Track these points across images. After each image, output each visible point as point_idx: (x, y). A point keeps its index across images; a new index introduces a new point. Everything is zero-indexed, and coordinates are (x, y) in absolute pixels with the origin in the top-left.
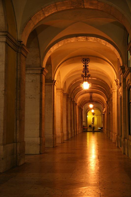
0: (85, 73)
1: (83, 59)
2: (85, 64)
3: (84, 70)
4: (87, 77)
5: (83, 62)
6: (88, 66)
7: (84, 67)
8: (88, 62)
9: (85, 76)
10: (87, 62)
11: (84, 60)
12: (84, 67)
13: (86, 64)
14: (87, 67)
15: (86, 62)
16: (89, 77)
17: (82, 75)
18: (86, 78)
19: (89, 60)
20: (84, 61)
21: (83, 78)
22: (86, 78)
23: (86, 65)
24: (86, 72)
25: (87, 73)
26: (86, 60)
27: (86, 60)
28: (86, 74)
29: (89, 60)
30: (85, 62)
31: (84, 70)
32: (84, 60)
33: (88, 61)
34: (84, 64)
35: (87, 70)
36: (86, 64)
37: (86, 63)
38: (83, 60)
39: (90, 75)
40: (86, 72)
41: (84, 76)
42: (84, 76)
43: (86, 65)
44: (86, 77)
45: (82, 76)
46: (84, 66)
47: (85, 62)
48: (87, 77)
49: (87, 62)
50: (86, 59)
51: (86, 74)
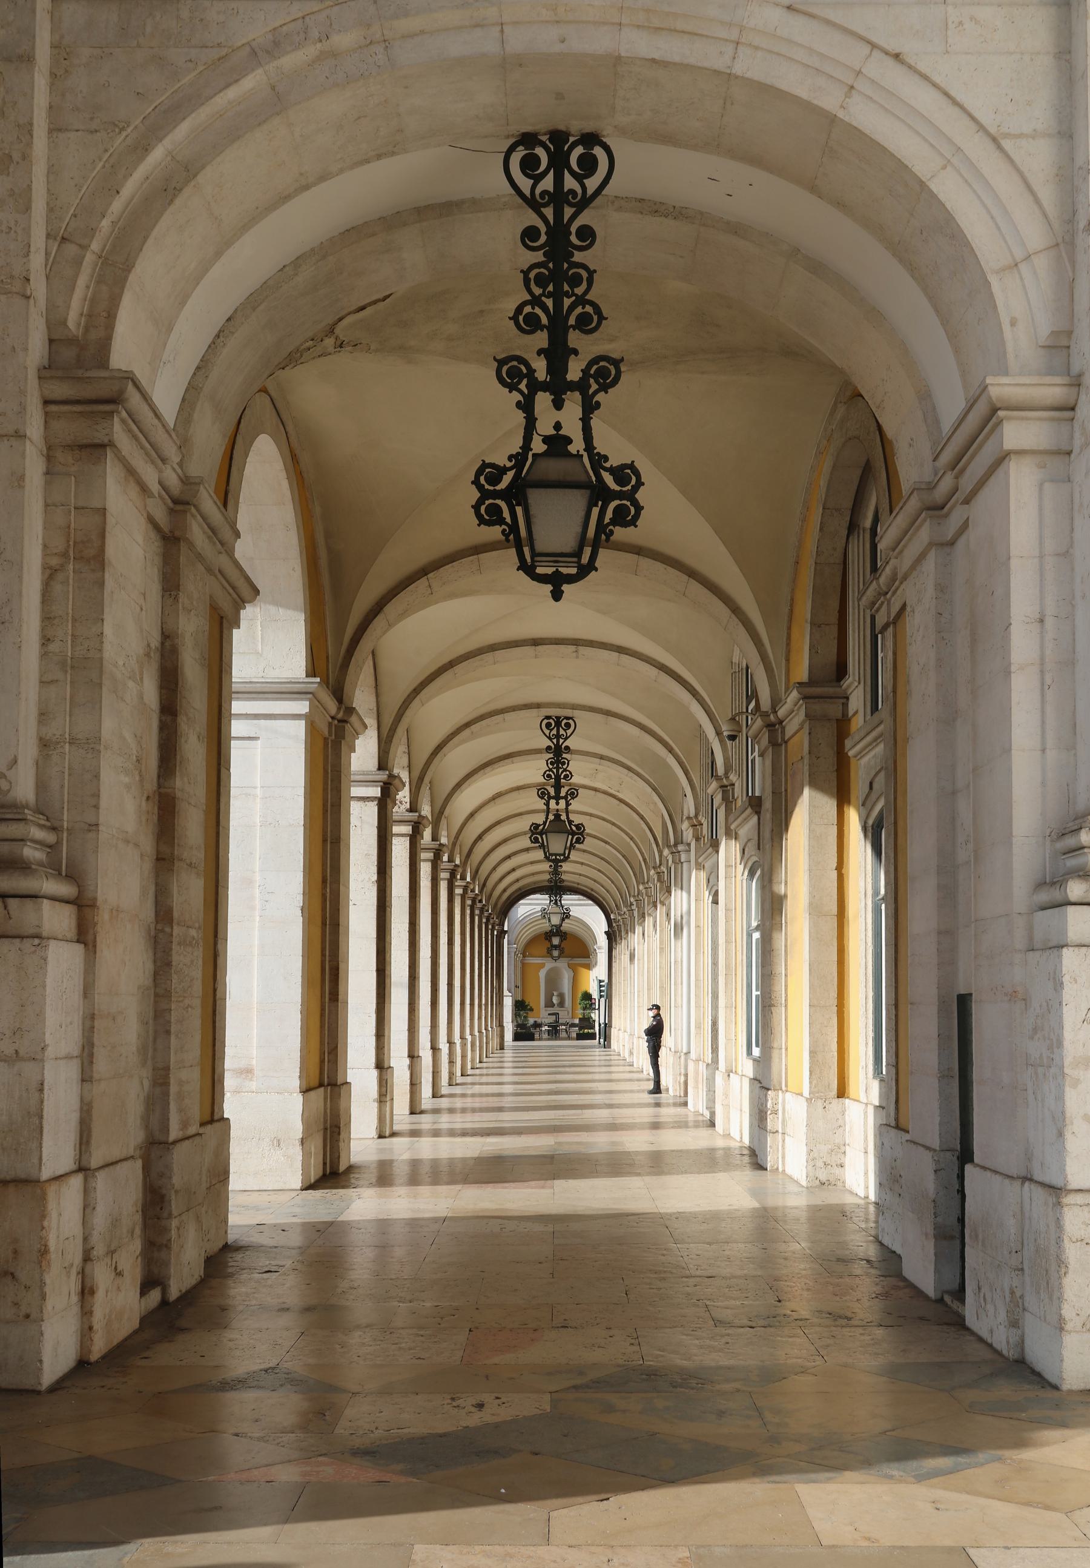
0: (541, 339)
1: (528, 139)
2: (549, 212)
3: (535, 301)
4: (581, 386)
6: (587, 234)
7: (539, 257)
8: (592, 183)
9: (541, 374)
10: (570, 183)
11: (540, 152)
12: (539, 257)
13: (558, 214)
14: (578, 257)
15: (559, 181)
16: (604, 388)
17: (501, 363)
18: (558, 405)
19: (598, 151)
20: (529, 165)
21: (527, 406)
22: (558, 405)
23: (558, 231)
24: (558, 329)
25: (574, 338)
26: (558, 162)
27: (558, 162)
28: (558, 354)
29: (598, 151)
31: (535, 301)
32: (540, 152)
33: (589, 165)
34: (533, 203)
35: (581, 301)
36: (568, 212)
37: (558, 197)
39: (616, 363)
40: (558, 329)
41: (535, 386)
42: (535, 386)
43: (558, 231)
44: (557, 798)
46: (529, 235)
47: (547, 183)
48: (581, 386)
49: (570, 183)
50: (558, 137)
51: (558, 354)
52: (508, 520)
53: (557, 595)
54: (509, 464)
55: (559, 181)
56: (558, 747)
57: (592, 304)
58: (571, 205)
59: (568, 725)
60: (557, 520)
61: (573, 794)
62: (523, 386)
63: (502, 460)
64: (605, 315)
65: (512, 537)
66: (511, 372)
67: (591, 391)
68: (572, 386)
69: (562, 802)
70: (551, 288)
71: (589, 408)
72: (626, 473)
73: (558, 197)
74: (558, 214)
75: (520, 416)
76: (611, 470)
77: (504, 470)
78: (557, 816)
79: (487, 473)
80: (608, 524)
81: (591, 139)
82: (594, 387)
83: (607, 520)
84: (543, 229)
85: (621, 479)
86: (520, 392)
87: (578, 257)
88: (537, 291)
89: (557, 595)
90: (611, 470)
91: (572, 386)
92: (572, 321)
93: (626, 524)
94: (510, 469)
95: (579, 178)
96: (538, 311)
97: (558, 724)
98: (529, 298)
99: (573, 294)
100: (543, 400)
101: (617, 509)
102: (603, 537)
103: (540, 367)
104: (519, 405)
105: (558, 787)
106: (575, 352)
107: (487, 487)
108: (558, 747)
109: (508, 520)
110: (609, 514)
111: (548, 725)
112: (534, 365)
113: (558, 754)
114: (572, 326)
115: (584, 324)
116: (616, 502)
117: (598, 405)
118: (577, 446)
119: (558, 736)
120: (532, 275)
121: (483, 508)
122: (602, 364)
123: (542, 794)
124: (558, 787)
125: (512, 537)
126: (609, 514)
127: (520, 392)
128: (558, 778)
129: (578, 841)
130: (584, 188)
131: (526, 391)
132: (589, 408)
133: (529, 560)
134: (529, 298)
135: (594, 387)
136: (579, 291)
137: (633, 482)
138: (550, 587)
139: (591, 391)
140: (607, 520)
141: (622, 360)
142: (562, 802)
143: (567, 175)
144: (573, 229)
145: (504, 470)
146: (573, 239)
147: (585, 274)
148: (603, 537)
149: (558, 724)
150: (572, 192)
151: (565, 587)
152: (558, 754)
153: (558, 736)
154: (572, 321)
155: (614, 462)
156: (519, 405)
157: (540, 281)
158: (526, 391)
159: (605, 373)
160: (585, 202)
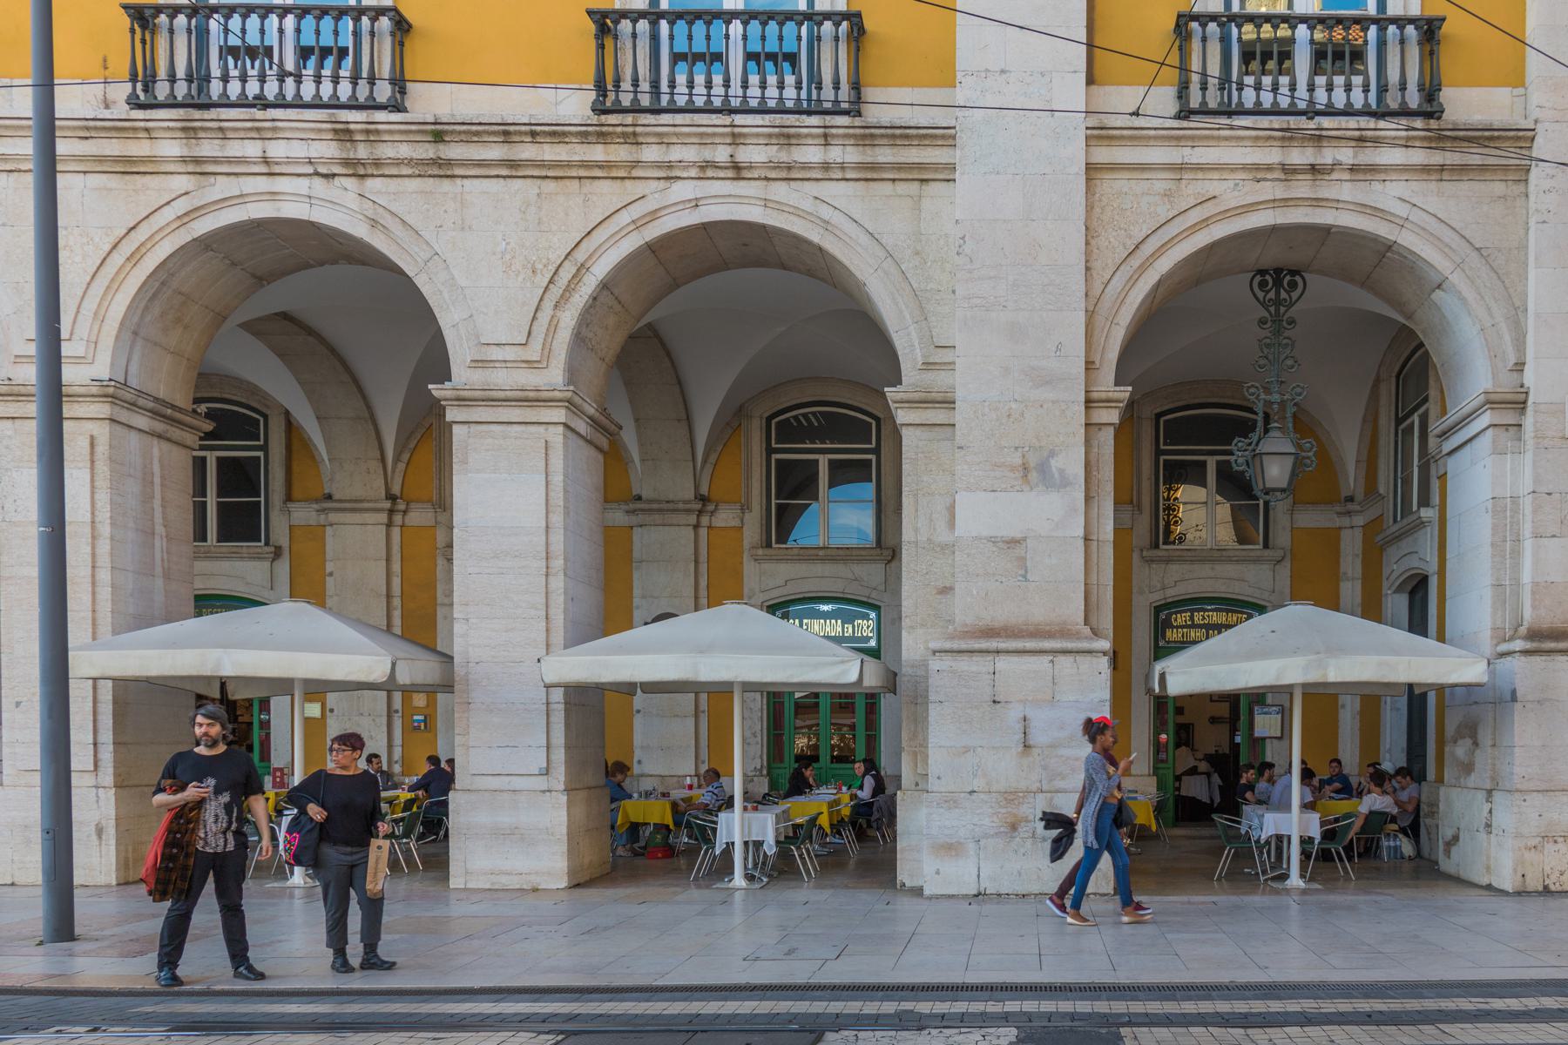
2: (1272, 309)
5: (1261, 295)
6: (1292, 322)
8: (1295, 295)
10: (1283, 295)
11: (1268, 277)
13: (1277, 310)
15: (1278, 293)
19: (1298, 278)
20: (1263, 285)
23: (1277, 319)
26: (1278, 283)
27: (1278, 283)
29: (1298, 278)
30: (1272, 295)
33: (1293, 285)
34: (1263, 304)
36: (1282, 309)
37: (1278, 302)
38: (1258, 278)
46: (1262, 322)
47: (1272, 295)
49: (1283, 295)
55: (1278, 293)
73: (1278, 302)
74: (1277, 310)
81: (1293, 273)
95: (1288, 292)
160: (1292, 304)
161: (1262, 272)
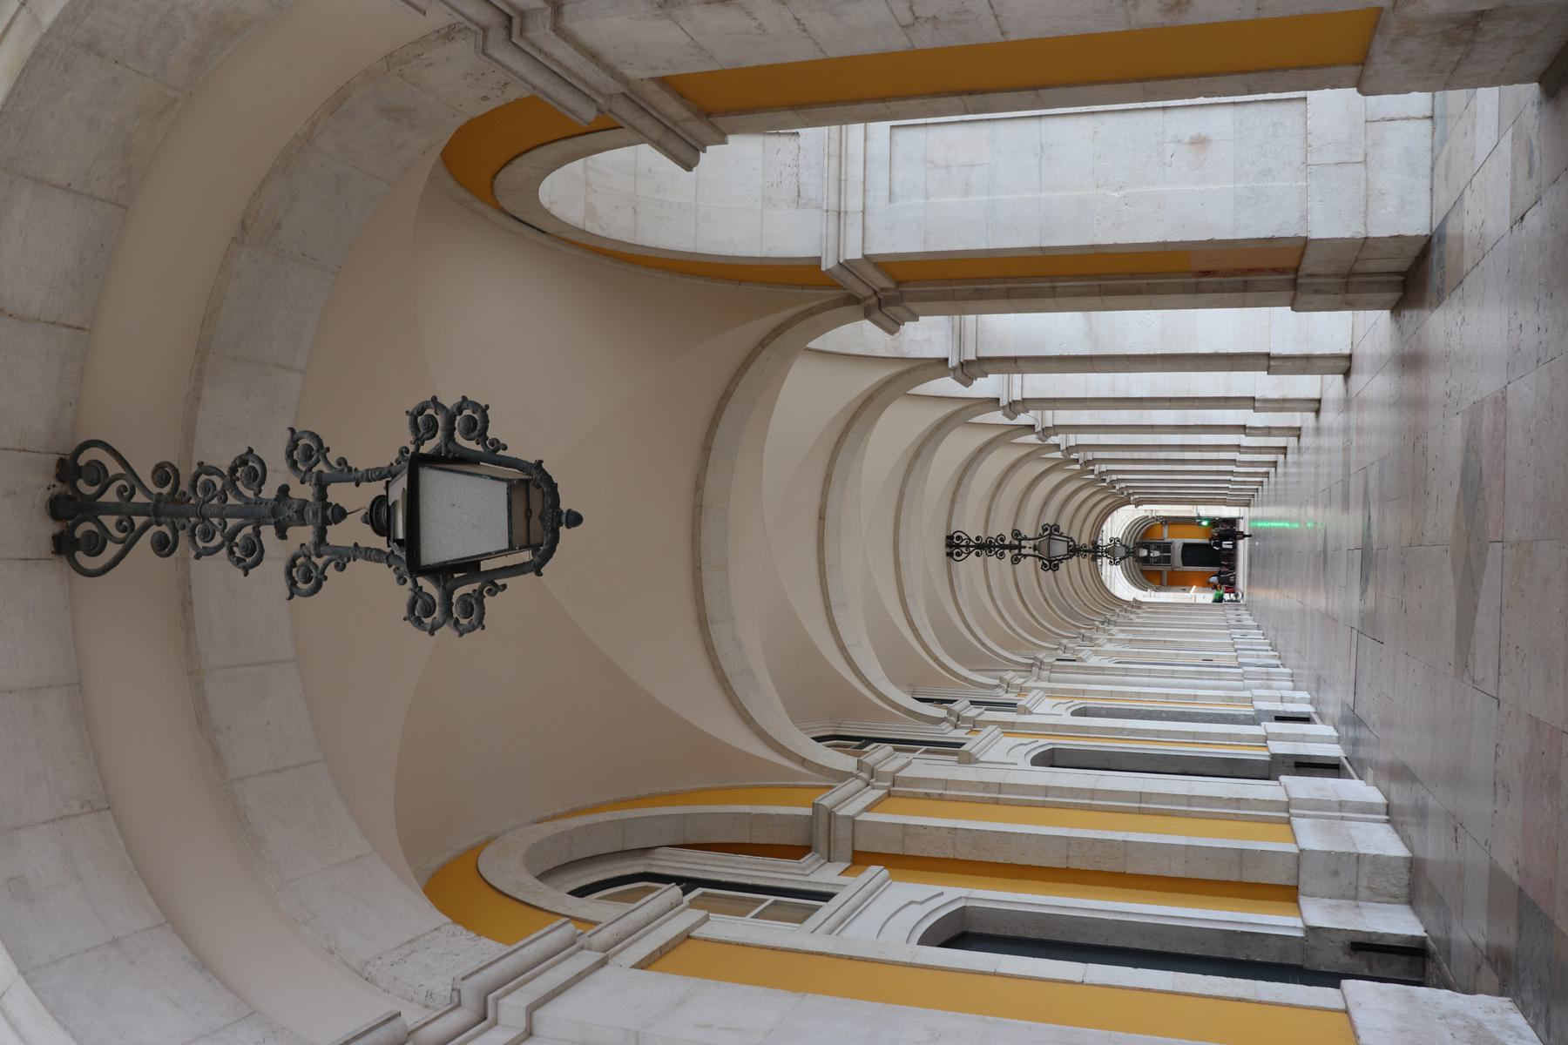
0: (268, 533)
2: (139, 521)
5: (112, 550)
6: (164, 473)
8: (114, 468)
13: (141, 510)
15: (110, 509)
16: (323, 450)
17: (293, 590)
18: (341, 514)
19: (83, 460)
20: (95, 545)
21: (342, 558)
22: (341, 514)
24: (255, 515)
26: (91, 508)
30: (110, 521)
33: (98, 474)
36: (139, 498)
40: (255, 515)
44: (1020, 547)
45: (1015, 560)
46: (164, 547)
47: (110, 521)
49: (111, 496)
51: (282, 513)
52: (476, 586)
53: (575, 519)
54: (409, 583)
55: (110, 509)
56: (978, 546)
57: (233, 470)
58: (133, 494)
59: (959, 538)
60: (466, 516)
61: (1016, 534)
62: (320, 562)
63: (405, 592)
64: (245, 450)
65: (499, 582)
66: (305, 578)
67: (326, 470)
68: (322, 495)
69: (1024, 543)
70: (215, 521)
71: (346, 473)
72: (423, 420)
75: (357, 567)
76: (419, 441)
77: (417, 590)
78: (1035, 548)
79: (419, 611)
80: (485, 446)
82: (321, 466)
83: (479, 448)
84: (154, 529)
85: (432, 426)
86: (326, 566)
87: (184, 486)
88: (218, 539)
89: (575, 519)
90: (419, 441)
91: (322, 495)
92: (249, 494)
93: (486, 421)
94: (415, 583)
96: (238, 540)
97: (958, 546)
98: (224, 551)
99: (223, 491)
100: (339, 535)
101: (467, 435)
102: (501, 452)
103: (302, 535)
104: (341, 567)
105: (1011, 547)
106: (284, 490)
107: (437, 614)
108: (978, 546)
109: (476, 586)
110: (471, 445)
111: (958, 554)
112: (295, 548)
113: (986, 547)
114: (256, 495)
115: (258, 477)
116: (457, 435)
117: (342, 461)
118: (378, 488)
119: (968, 546)
120: (201, 544)
121: (464, 621)
122: (295, 456)
123: (1015, 560)
124: (1011, 547)
125: (499, 582)
126: (471, 445)
127: (326, 566)
128: (1004, 547)
129: (1057, 529)
130: (118, 477)
131: (325, 558)
132: (346, 473)
133: (526, 556)
134: (224, 551)
135: (321, 466)
136: (219, 483)
137: (430, 411)
138: (563, 529)
139: (326, 470)
140: (479, 448)
141: (292, 430)
142: (1024, 543)
143: (102, 499)
144: (155, 490)
145: (417, 590)
146: (166, 490)
147: (203, 477)
148: (501, 452)
149: (958, 546)
150: (120, 492)
151: (564, 507)
152: (986, 547)
153: (968, 546)
154: (249, 494)
155: (406, 439)
156: (341, 567)
157: (208, 535)
158: (325, 558)
159: (306, 451)
161: (950, 555)
